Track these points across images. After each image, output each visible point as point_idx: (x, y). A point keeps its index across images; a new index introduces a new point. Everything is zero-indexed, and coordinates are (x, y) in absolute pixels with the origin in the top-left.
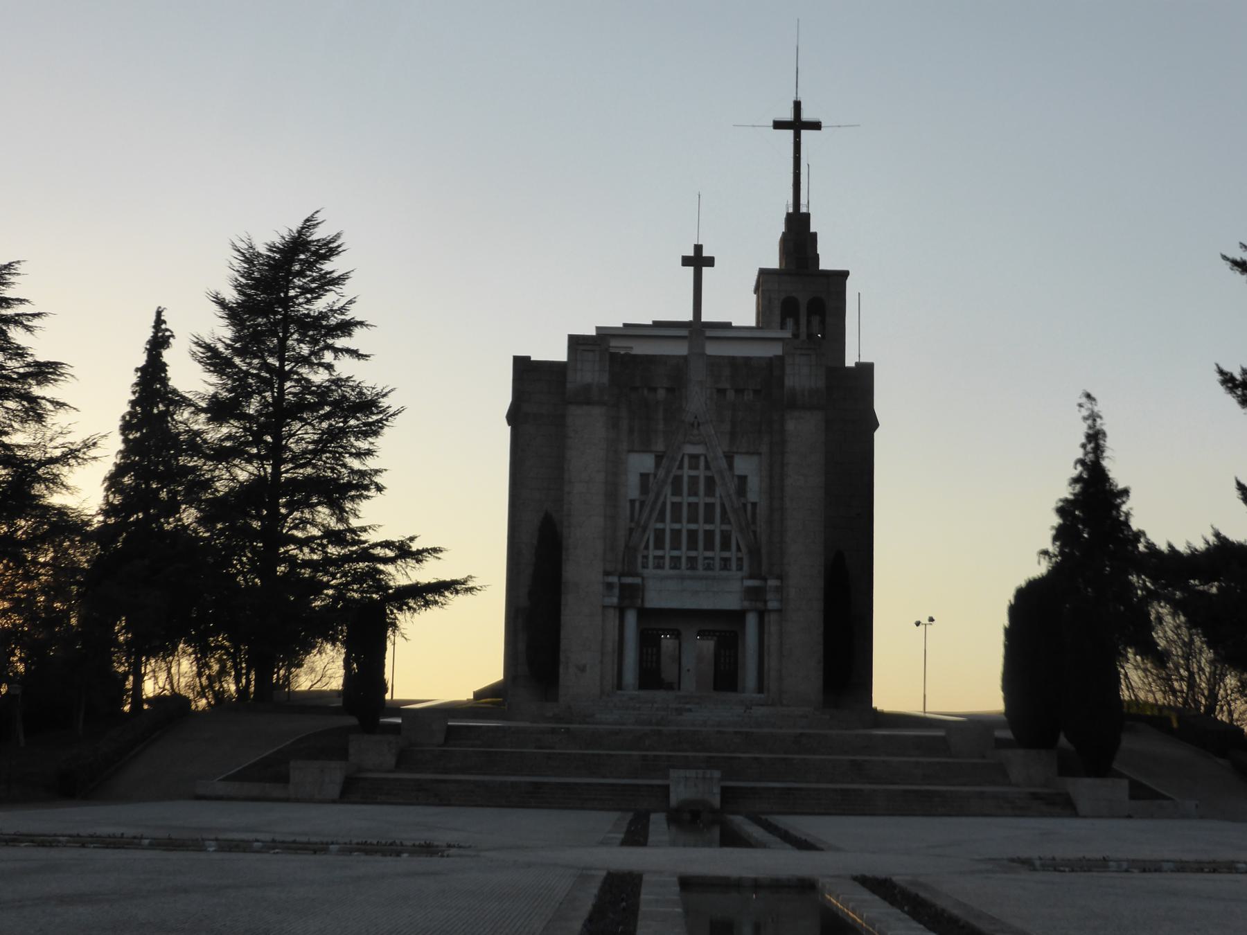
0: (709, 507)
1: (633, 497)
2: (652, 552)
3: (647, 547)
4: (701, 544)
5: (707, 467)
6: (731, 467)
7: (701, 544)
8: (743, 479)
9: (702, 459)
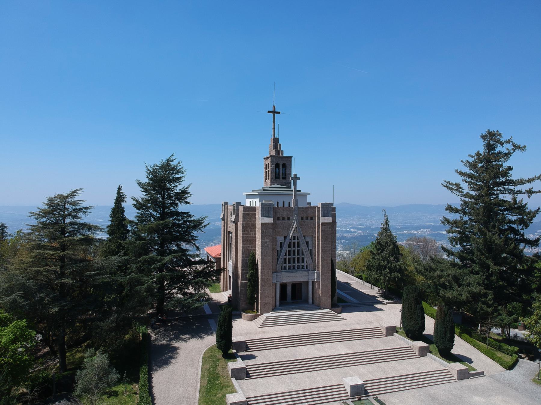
0: (298, 251)
1: (278, 249)
2: (283, 265)
3: (282, 264)
4: (296, 262)
5: (298, 239)
6: (305, 241)
7: (296, 262)
8: (307, 243)
9: (297, 237)
